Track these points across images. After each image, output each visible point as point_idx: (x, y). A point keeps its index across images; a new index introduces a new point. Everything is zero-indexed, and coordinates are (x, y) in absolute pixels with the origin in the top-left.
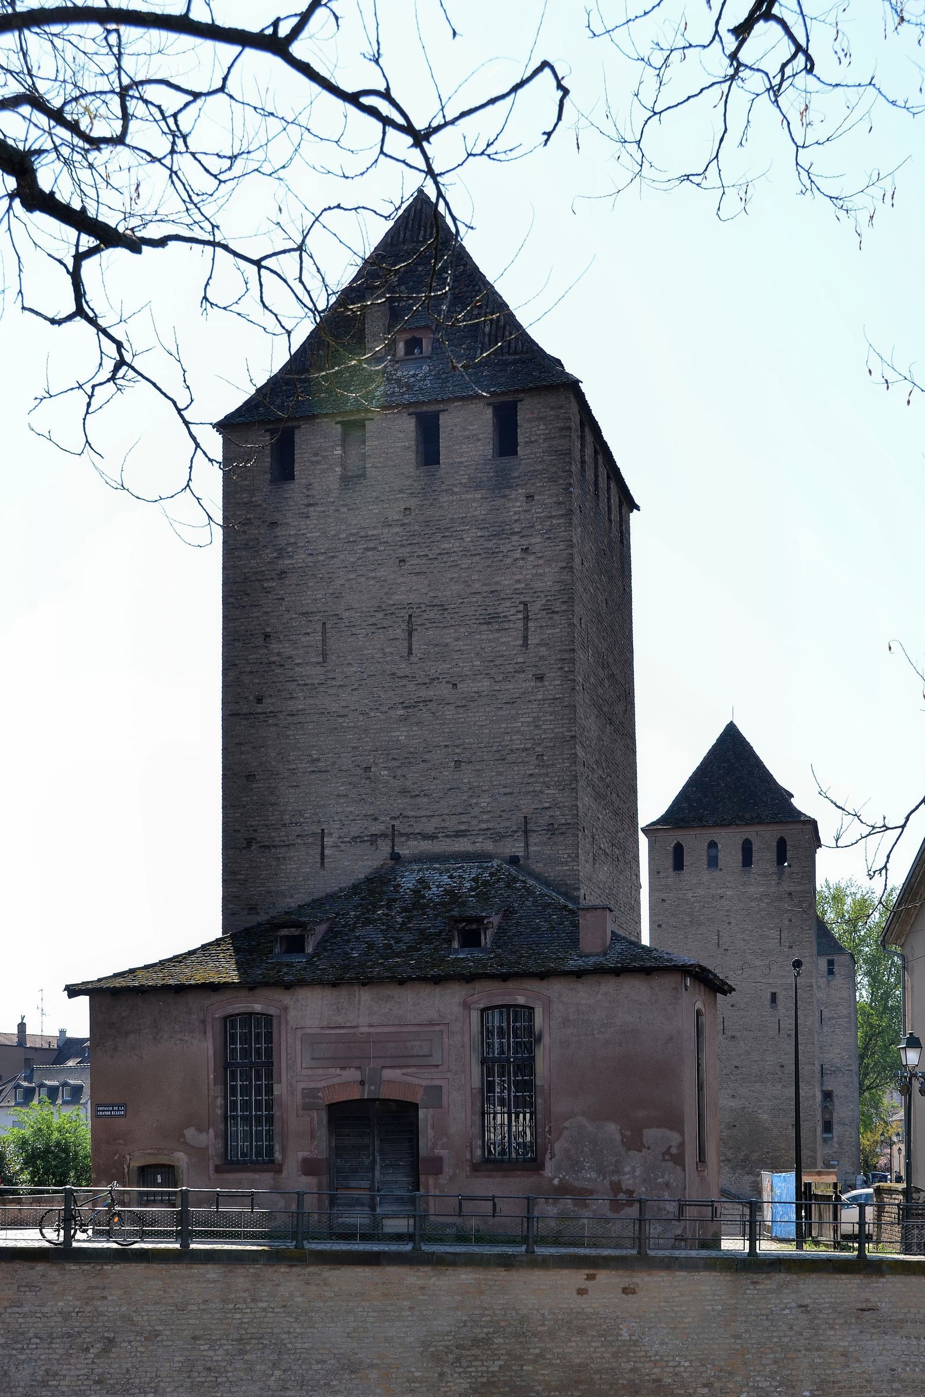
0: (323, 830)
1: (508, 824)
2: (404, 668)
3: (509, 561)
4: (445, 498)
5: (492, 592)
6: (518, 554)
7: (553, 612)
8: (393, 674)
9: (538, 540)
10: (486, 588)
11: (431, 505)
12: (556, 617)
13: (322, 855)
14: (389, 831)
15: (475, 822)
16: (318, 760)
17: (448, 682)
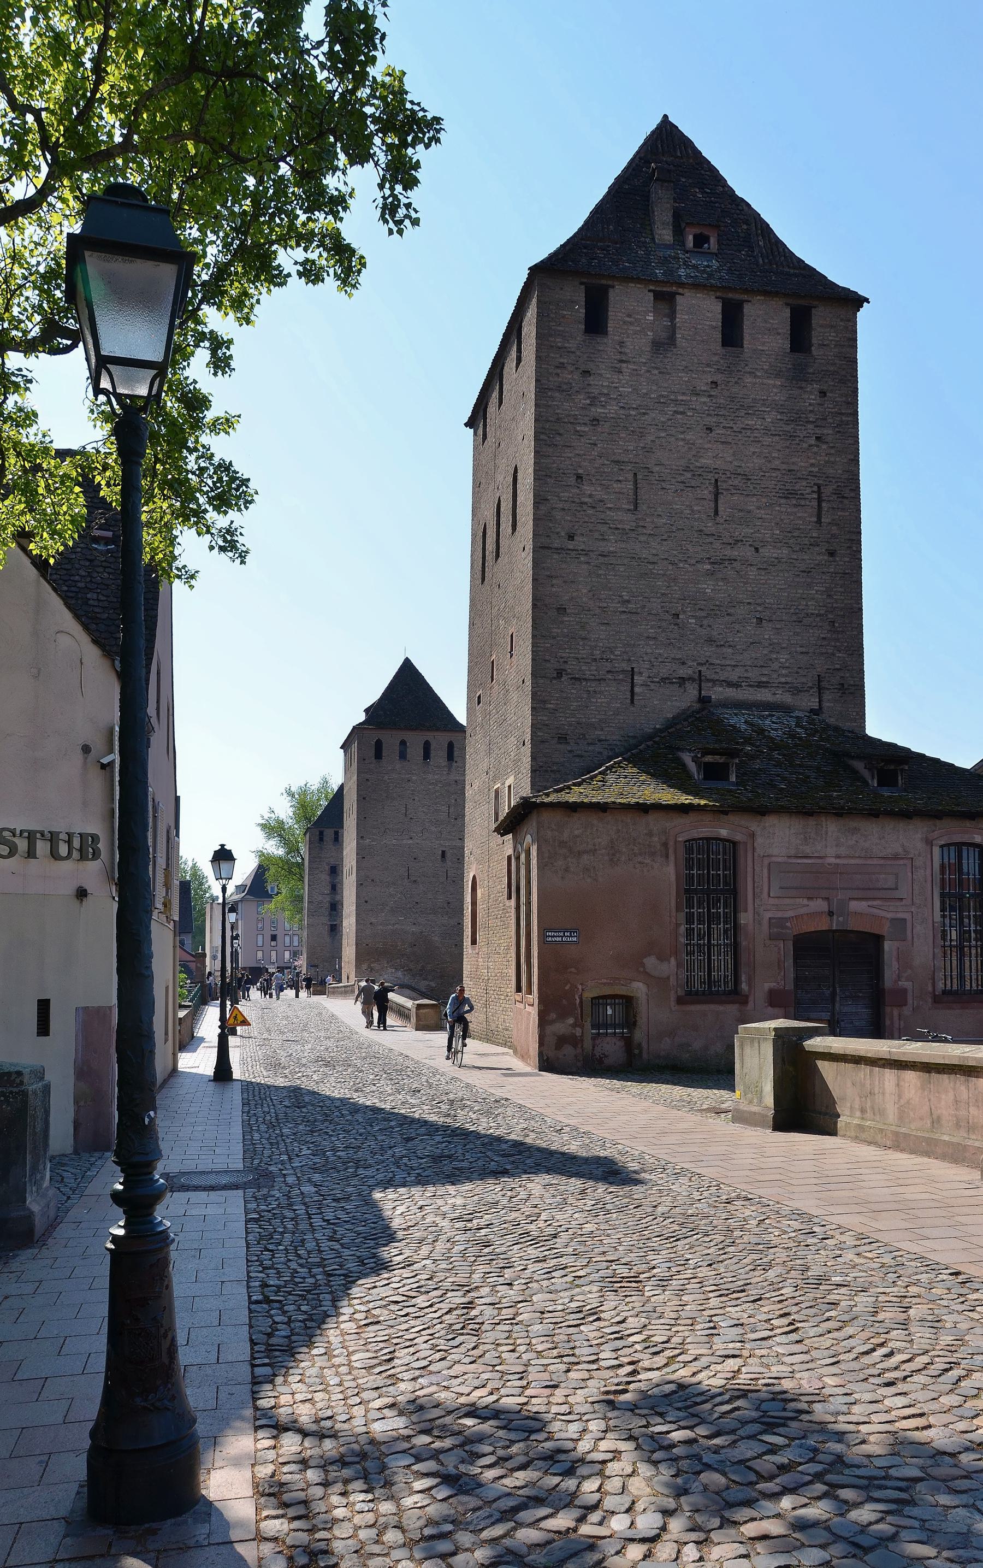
0: (633, 668)
1: (804, 680)
2: (710, 527)
3: (805, 445)
4: (748, 380)
5: (789, 471)
6: (813, 441)
7: (843, 497)
8: (701, 531)
9: (830, 432)
10: (784, 466)
11: (736, 383)
12: (846, 501)
13: (632, 693)
14: (696, 676)
15: (775, 676)
16: (628, 601)
17: (751, 545)
